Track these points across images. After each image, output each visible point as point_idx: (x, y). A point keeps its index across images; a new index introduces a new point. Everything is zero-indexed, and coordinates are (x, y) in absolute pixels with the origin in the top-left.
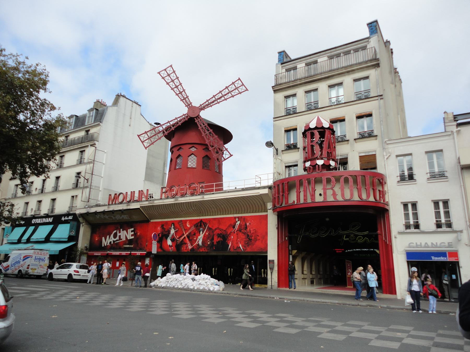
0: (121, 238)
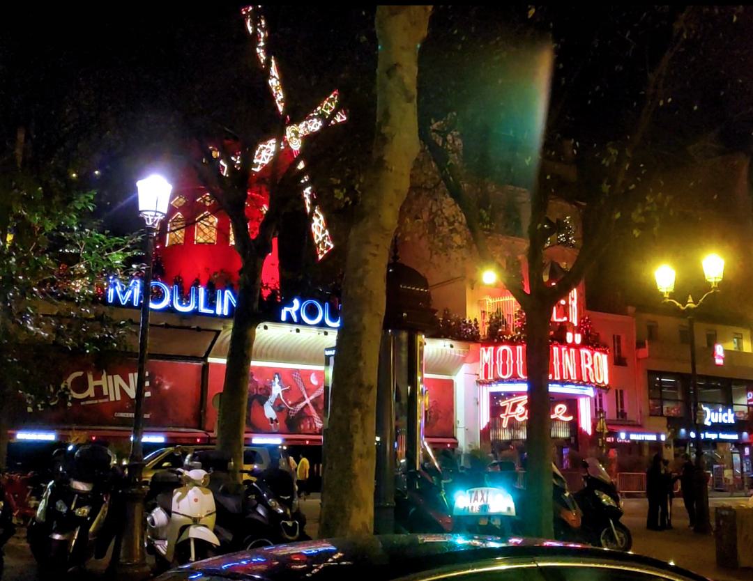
0: (105, 393)
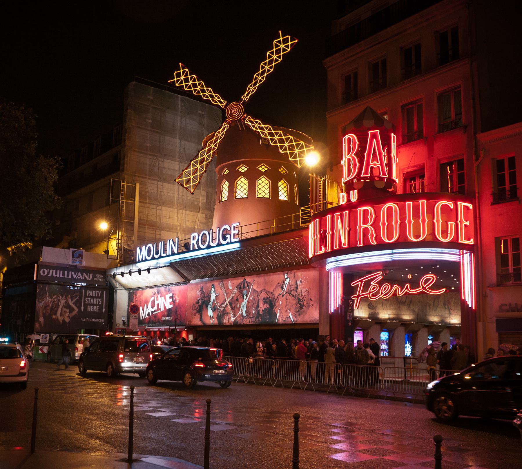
0: (159, 308)
